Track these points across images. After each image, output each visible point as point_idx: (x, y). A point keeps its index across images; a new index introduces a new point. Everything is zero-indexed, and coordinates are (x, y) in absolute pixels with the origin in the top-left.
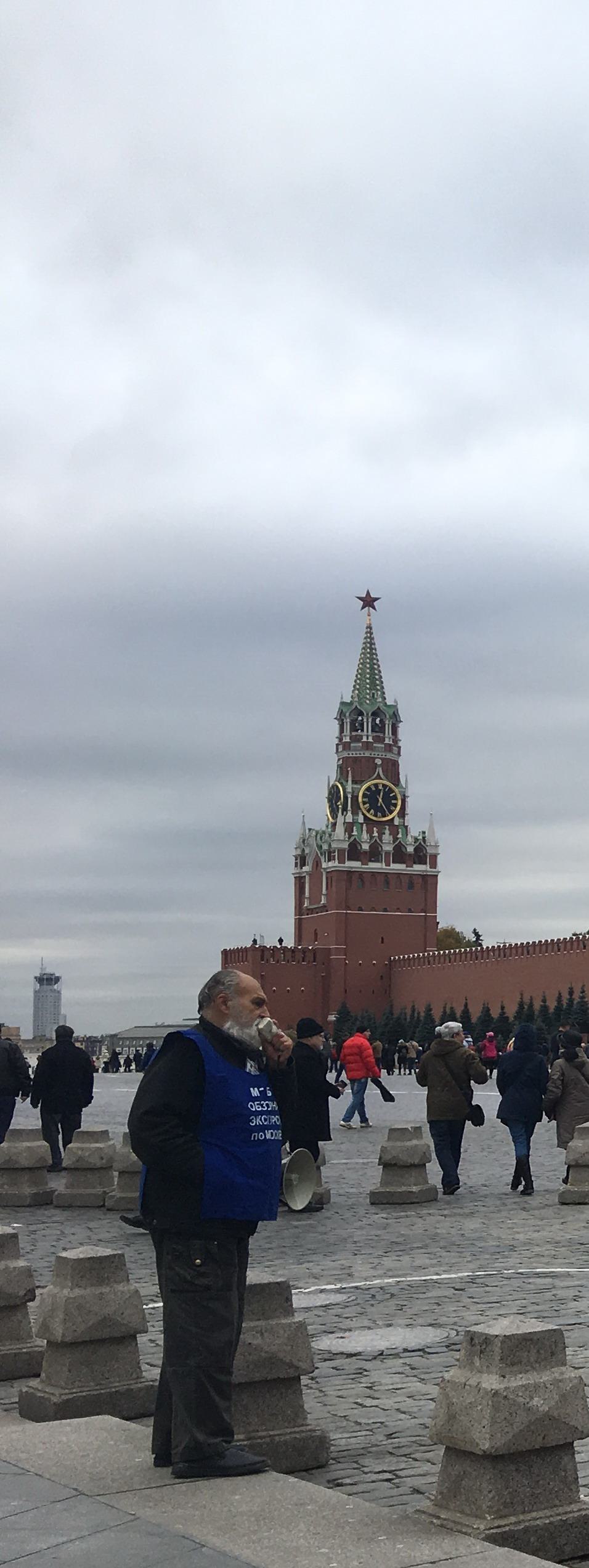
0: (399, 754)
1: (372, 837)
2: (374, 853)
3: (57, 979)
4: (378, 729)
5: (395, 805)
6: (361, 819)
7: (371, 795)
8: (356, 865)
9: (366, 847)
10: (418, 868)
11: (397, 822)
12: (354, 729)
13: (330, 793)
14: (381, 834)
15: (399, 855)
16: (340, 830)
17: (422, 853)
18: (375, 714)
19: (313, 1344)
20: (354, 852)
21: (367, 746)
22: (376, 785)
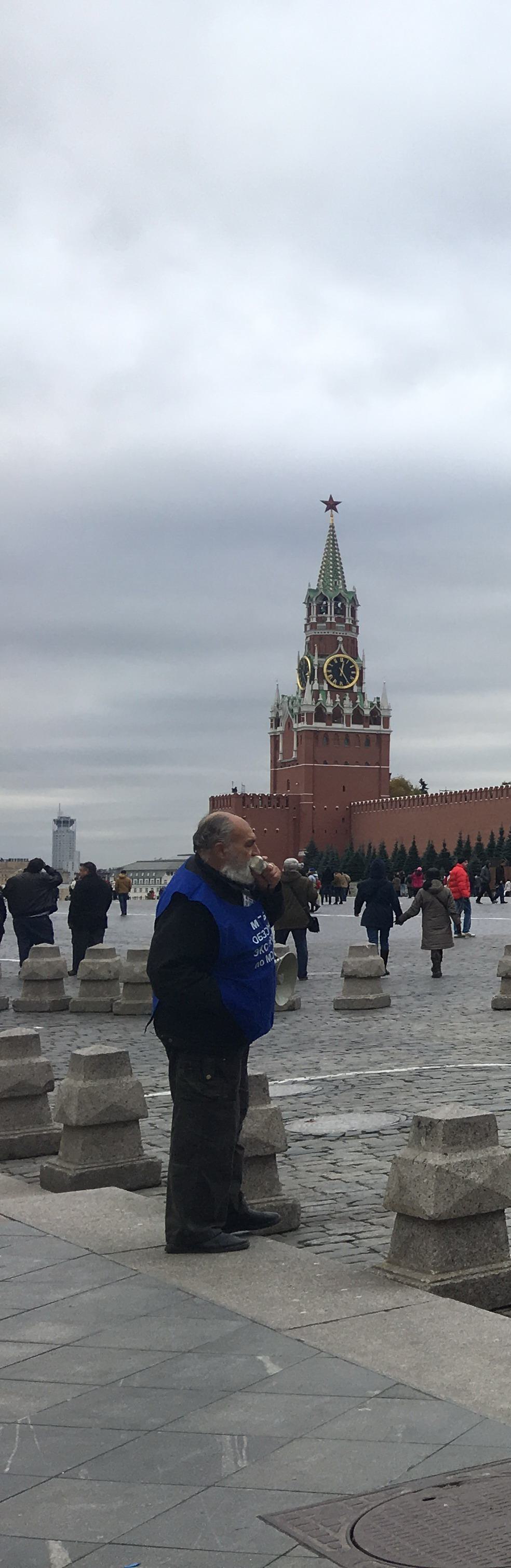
0: (357, 632)
1: (335, 702)
2: (337, 716)
3: (72, 822)
4: (340, 611)
5: (354, 676)
6: (326, 687)
7: (335, 667)
8: (321, 726)
9: (330, 710)
10: (374, 728)
11: (355, 690)
12: (319, 611)
13: (300, 665)
14: (343, 700)
15: (358, 717)
16: (308, 697)
17: (377, 716)
18: (337, 599)
19: (286, 1127)
20: (320, 715)
21: (331, 626)
22: (338, 659)
